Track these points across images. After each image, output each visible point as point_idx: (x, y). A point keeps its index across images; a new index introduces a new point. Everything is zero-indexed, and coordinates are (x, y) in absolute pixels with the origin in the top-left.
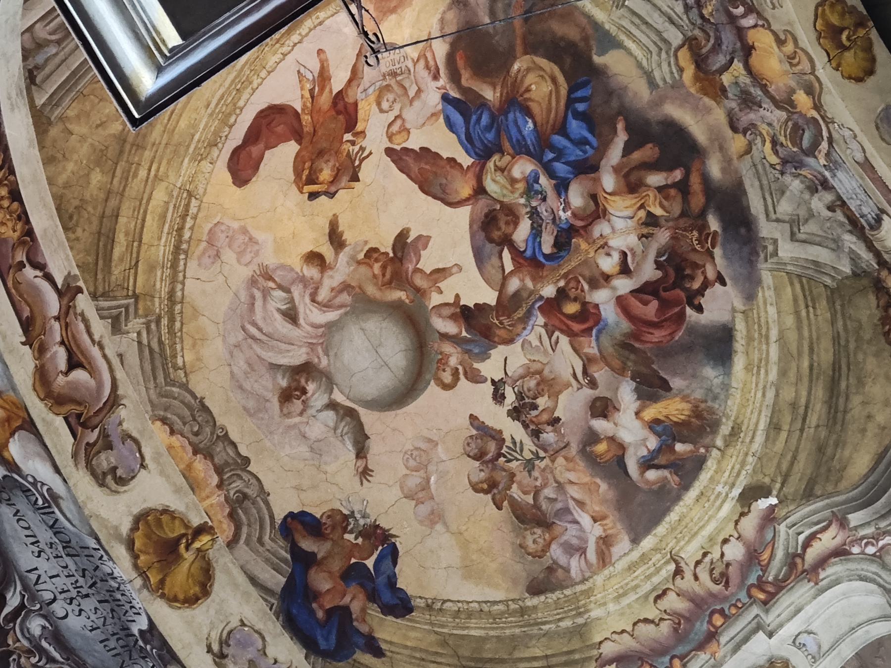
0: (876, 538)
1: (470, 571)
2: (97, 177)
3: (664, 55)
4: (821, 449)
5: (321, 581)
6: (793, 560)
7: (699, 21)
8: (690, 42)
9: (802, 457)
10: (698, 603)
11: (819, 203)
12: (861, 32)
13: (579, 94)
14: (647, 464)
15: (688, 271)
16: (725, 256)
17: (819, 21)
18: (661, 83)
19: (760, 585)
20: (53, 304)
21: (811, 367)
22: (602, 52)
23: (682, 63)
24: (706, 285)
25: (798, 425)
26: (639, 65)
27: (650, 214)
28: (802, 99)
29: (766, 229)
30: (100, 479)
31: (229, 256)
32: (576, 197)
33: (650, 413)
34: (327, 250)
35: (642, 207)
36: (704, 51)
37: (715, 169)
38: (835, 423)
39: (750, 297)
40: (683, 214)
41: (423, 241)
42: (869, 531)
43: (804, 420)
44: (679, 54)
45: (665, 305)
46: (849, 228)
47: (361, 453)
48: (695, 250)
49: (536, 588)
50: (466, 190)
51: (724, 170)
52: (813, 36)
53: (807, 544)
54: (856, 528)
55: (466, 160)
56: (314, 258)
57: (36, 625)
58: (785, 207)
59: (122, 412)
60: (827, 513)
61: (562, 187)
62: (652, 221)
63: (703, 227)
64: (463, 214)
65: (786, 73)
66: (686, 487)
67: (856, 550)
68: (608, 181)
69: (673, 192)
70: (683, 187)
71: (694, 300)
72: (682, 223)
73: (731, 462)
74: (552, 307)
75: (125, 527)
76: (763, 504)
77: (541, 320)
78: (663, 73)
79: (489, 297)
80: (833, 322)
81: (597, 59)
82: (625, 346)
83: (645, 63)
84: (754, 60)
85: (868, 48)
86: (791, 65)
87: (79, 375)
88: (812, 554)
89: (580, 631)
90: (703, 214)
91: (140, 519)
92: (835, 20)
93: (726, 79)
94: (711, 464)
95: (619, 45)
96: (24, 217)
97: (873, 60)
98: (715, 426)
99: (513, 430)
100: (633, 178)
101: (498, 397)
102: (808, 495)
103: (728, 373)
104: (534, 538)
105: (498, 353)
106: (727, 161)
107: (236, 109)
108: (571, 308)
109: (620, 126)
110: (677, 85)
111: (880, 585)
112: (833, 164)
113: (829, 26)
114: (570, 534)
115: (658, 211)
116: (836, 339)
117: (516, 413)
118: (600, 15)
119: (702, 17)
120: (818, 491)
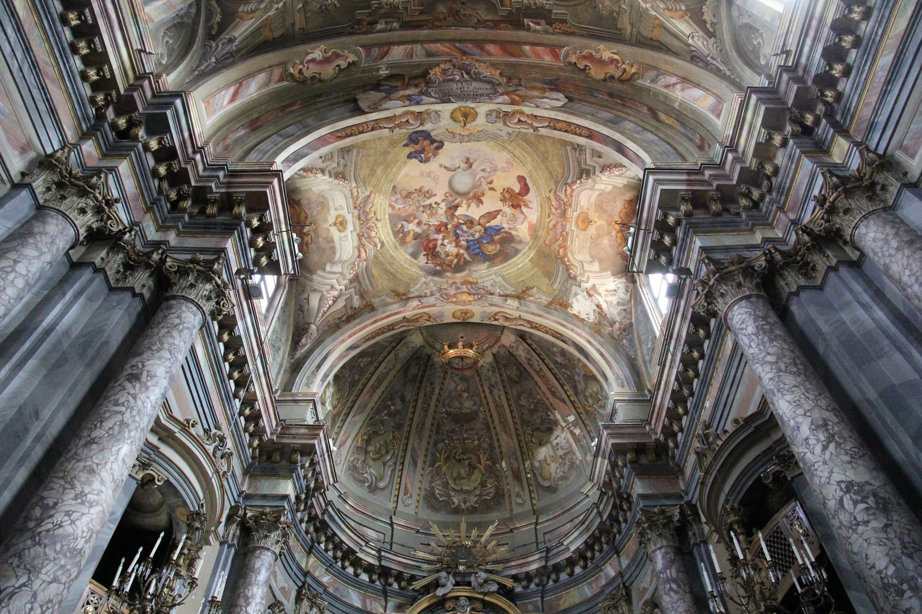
1: (407, 175)
2: (543, 149)
4: (382, 264)
5: (426, 143)
6: (363, 245)
8: (476, 283)
10: (368, 220)
11: (428, 292)
14: (402, 226)
19: (363, 235)
20: (536, 125)
28: (454, 300)
29: (430, 278)
30: (491, 111)
31: (506, 165)
32: (463, 243)
33: (412, 233)
34: (491, 186)
37: (449, 274)
39: (420, 268)
41: (478, 206)
45: (430, 249)
47: (445, 167)
49: (394, 187)
50: (482, 221)
55: (487, 225)
56: (491, 182)
57: (457, 77)
58: (431, 284)
59: (501, 124)
61: (468, 241)
62: (448, 255)
63: (439, 265)
64: (477, 218)
66: (393, 231)
68: (462, 251)
70: (449, 266)
71: (427, 255)
73: (391, 243)
74: (446, 225)
75: (477, 110)
76: (379, 246)
77: (445, 221)
79: (457, 213)
82: (428, 236)
87: (517, 120)
88: (362, 250)
89: (380, 191)
91: (477, 114)
94: (393, 239)
96: (560, 130)
98: (400, 245)
99: (428, 202)
101: (436, 203)
102: (375, 257)
104: (404, 193)
105: (444, 208)
107: (535, 184)
108: (443, 229)
110: (470, 276)
112: (437, 299)
114: (400, 201)
117: (430, 205)
118: (495, 268)
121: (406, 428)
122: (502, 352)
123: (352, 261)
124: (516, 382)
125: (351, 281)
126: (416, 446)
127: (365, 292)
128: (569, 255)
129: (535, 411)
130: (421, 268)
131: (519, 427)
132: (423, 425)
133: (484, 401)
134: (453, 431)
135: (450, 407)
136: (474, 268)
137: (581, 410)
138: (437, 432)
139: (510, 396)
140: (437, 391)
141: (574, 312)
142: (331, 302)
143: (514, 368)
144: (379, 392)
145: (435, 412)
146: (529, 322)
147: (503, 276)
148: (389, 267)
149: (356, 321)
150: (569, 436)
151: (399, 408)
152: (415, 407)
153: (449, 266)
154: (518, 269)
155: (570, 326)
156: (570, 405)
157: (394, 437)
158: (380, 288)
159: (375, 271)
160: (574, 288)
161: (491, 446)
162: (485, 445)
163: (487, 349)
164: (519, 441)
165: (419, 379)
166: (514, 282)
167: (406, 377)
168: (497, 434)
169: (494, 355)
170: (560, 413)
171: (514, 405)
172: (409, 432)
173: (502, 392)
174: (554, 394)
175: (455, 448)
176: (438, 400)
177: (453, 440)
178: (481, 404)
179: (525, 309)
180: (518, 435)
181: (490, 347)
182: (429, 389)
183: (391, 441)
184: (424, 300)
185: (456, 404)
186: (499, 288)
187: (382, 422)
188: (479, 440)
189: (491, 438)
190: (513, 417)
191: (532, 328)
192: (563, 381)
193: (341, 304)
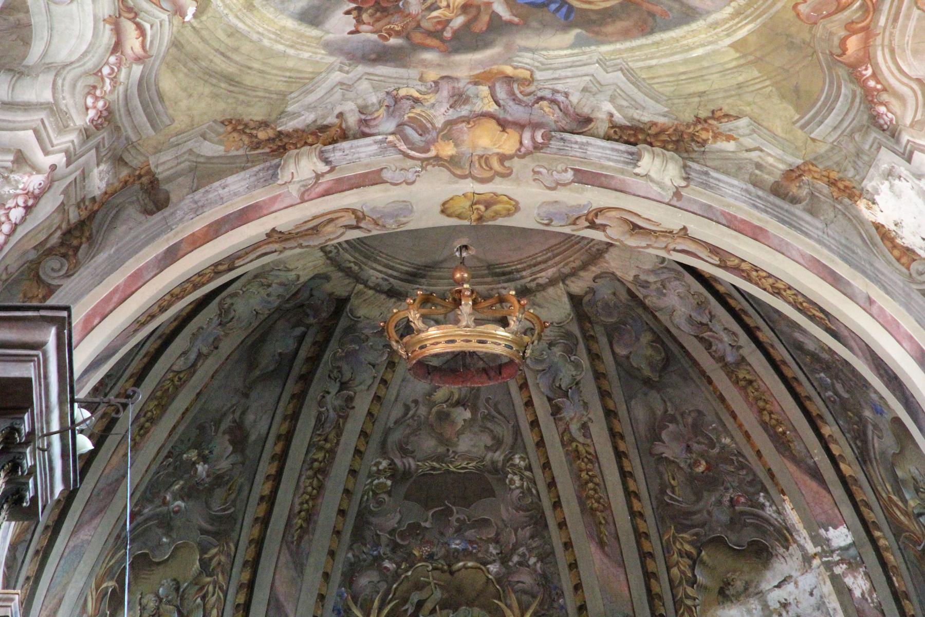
0: (114, 80)
3: (537, 64)
6: (133, 13)
7: (540, 94)
8: (531, 81)
9: (200, 46)
12: (474, 216)
13: (564, 10)
15: (378, 14)
16: (368, 40)
17: (506, 199)
18: (520, 54)
21: (250, 68)
22: (577, 36)
23: (519, 71)
24: (359, 21)
25: (222, 49)
26: (546, 49)
27: (439, 8)
28: (448, 150)
29: (361, 69)
35: (448, 6)
36: (515, 86)
37: (428, 56)
38: (205, 73)
39: (332, 48)
40: (418, 26)
42: (122, 76)
43: (223, 54)
44: (529, 72)
46: (319, 122)
48: (389, 23)
51: (423, 61)
52: (499, 192)
53: (139, 27)
54: (130, 68)
60: (154, 52)
63: (398, 34)
65: (475, 147)
67: (112, 59)
69: (439, 27)
70: (435, 34)
72: (414, 24)
78: (526, 59)
80: (266, 90)
81: (578, 31)
83: (544, 53)
84: (493, 124)
85: (459, 216)
86: (481, 157)
88: (130, 29)
90: (408, 37)
92: (497, 207)
93: (484, 90)
95: (572, 46)
97: (449, 216)
100: (473, 12)
102: (176, 44)
103: (292, 16)
106: (425, 64)
109: (516, 20)
110: (509, 61)
111: (72, 63)
113: (495, 203)
115: (435, 14)
116: (254, 89)
118: (605, 48)
119: (542, 98)
120: (173, 50)
121: (248, 531)
122: (605, 291)
123: (90, 63)
124: (647, 382)
125: (87, 134)
126: (282, 589)
127: (130, 145)
128: (881, 57)
129: (711, 481)
130: (332, 48)
131: (650, 525)
132: (310, 517)
133: (530, 438)
134: (415, 529)
135: (404, 451)
136: (521, 41)
137: (876, 515)
138: (358, 535)
139: (623, 426)
140: (363, 404)
141: (881, 219)
142: (16, 214)
143: (646, 338)
144: (159, 434)
145: (353, 472)
146: (714, 250)
147: (629, 73)
148: (221, 64)
149: (102, 257)
150: (827, 588)
151: (224, 465)
152: (282, 458)
153: (435, 34)
154: (686, 62)
155: (859, 283)
156: (838, 491)
157: (204, 564)
158: (181, 122)
159: (168, 84)
160: (886, 159)
161: (547, 582)
162: (526, 579)
163: (552, 282)
164: (648, 576)
165: (299, 367)
166: (668, 90)
167: (252, 366)
168: (568, 545)
169: (575, 300)
170: (796, 507)
171: (633, 453)
172: (259, 543)
173: (597, 413)
174: (782, 443)
175: (419, 586)
176: (364, 434)
177: (411, 560)
178: (517, 443)
179: (705, 198)
180: (645, 556)
181: (563, 278)
182: (332, 401)
183: (195, 581)
184: (342, 152)
185: (428, 444)
186: (612, 100)
187: (166, 523)
188: (504, 559)
189: (546, 556)
190: (630, 495)
191: (723, 266)
192: (817, 406)
193: (47, 207)
